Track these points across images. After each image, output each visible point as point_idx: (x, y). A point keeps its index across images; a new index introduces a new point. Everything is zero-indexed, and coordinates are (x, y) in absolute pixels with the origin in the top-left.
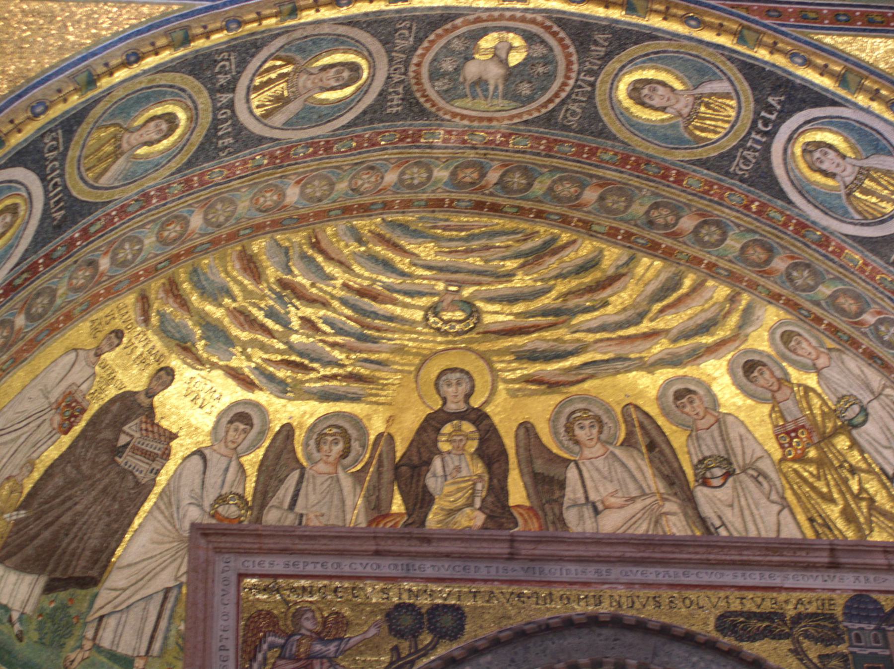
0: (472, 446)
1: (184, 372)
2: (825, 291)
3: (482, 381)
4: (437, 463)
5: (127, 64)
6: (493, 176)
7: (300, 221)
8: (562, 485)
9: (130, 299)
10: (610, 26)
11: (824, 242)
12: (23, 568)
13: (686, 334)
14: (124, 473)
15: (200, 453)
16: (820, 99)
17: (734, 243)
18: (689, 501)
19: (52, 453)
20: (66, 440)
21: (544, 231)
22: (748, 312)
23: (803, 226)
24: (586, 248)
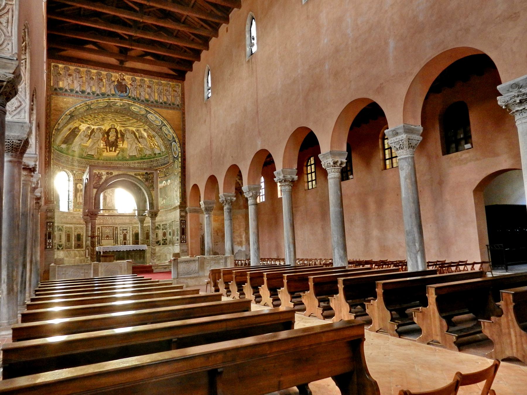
0: (115, 131)
1: (83, 124)
2: (152, 127)
3: (116, 125)
4: (111, 132)
5: (80, 106)
6: (118, 111)
7: (96, 113)
8: (124, 136)
9: (77, 120)
10: (131, 104)
11: (152, 123)
12: (64, 144)
13: (138, 126)
14: (75, 134)
15: (84, 131)
16: (152, 114)
17: (143, 121)
18: (138, 139)
19: (68, 133)
20: (69, 132)
21: (124, 115)
22: (145, 126)
23: (150, 122)
24: (128, 117)
